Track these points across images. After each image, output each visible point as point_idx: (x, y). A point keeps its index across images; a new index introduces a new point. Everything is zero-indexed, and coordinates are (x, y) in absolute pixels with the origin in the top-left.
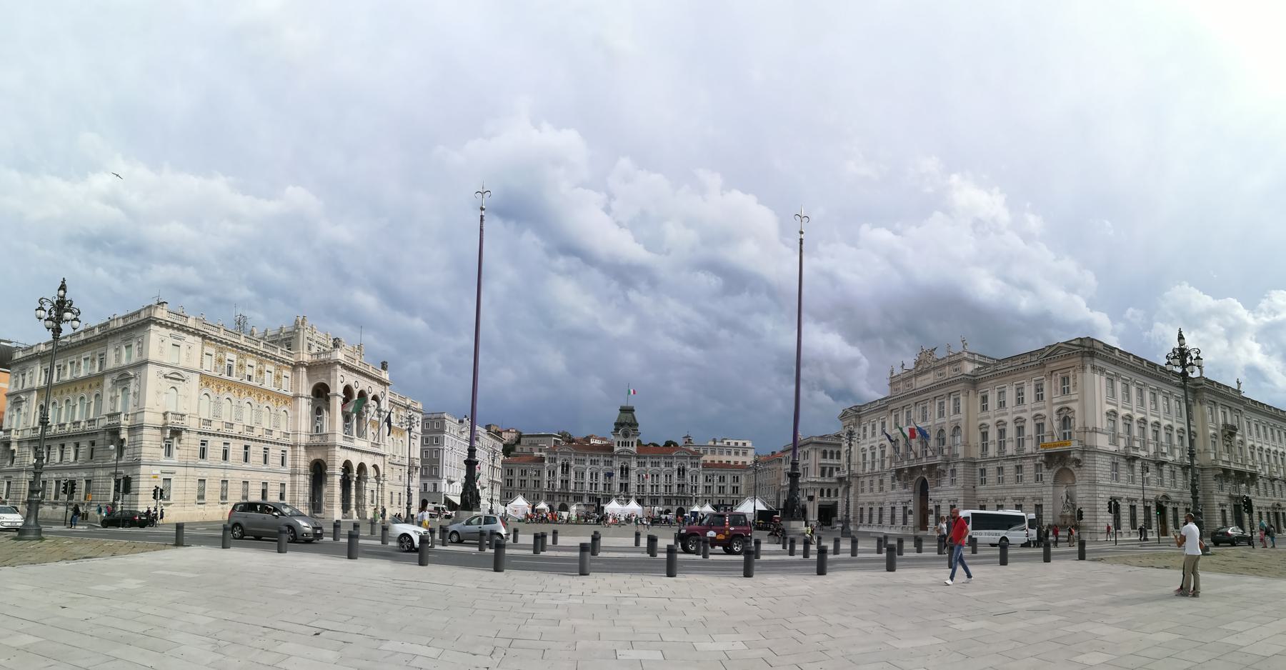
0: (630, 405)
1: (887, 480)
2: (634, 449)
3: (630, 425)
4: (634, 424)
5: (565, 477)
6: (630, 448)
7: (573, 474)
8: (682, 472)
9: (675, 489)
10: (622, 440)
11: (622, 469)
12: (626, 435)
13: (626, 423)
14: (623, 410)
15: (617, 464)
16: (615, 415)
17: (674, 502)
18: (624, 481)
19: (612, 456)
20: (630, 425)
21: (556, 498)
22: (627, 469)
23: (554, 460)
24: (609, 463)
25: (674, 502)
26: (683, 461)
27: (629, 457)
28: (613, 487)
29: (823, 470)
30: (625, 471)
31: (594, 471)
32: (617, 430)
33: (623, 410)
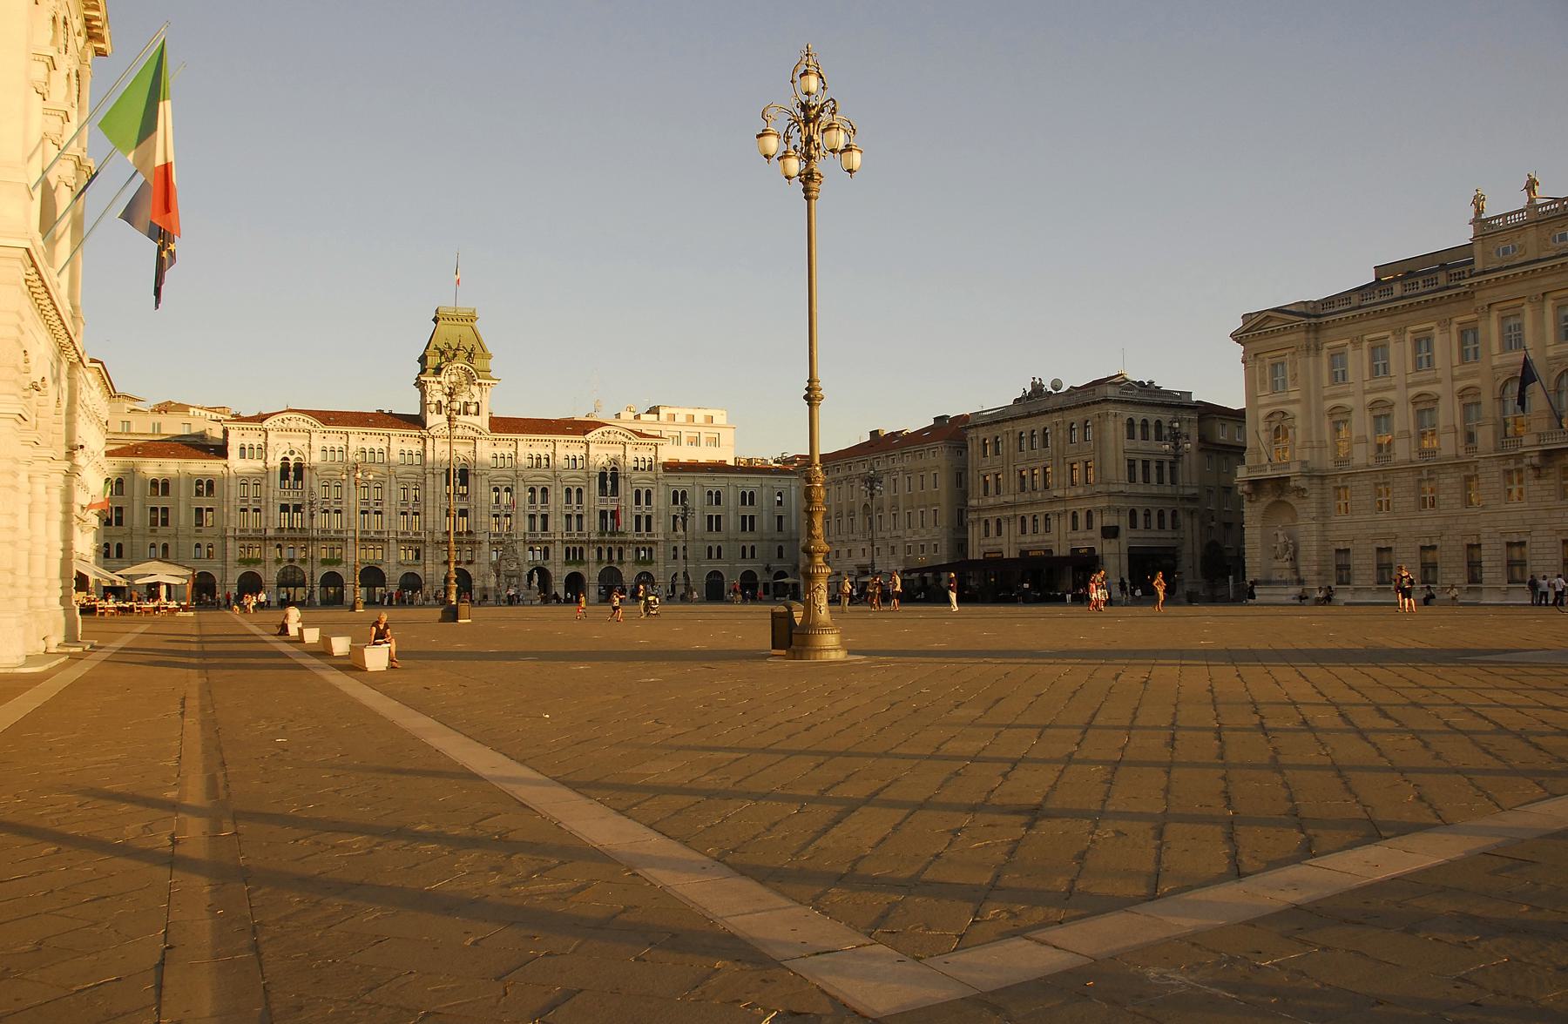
1: (1491, 476)
2: (483, 421)
9: (592, 524)
17: (591, 554)
25: (591, 554)
29: (1131, 465)
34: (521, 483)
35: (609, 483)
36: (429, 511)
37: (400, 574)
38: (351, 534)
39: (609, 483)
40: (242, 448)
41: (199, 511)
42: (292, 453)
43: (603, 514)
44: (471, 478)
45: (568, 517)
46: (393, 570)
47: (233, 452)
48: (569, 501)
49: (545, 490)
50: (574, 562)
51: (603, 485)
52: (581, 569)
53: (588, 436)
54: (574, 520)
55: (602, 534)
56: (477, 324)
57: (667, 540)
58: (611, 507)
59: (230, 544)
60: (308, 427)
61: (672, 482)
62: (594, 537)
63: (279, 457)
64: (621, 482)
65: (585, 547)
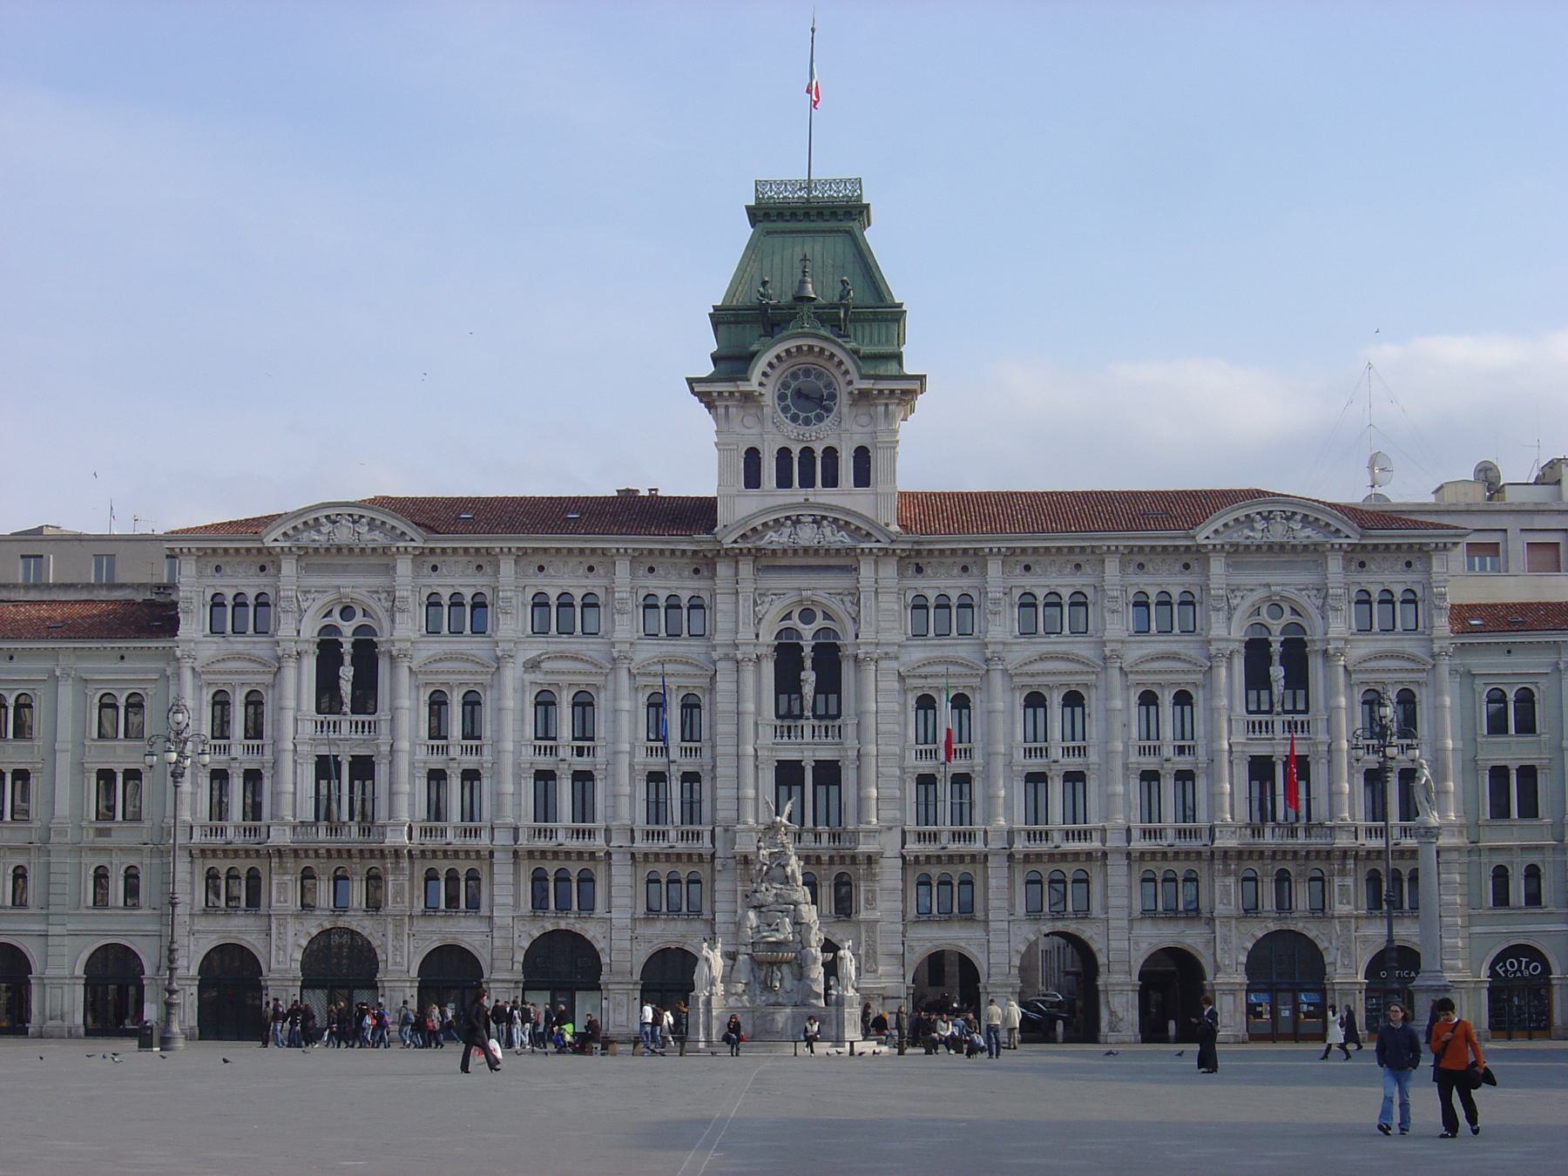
0: (831, 168)
3: (836, 319)
4: (868, 314)
5: (347, 741)
6: (845, 496)
7: (404, 703)
8: (1279, 664)
9: (1227, 801)
10: (775, 434)
11: (787, 656)
12: (809, 400)
13: (809, 311)
14: (769, 215)
15: (749, 616)
16: (715, 260)
18: (808, 750)
19: (704, 564)
20: (836, 319)
21: (282, 891)
22: (829, 658)
23: (255, 613)
24: (681, 618)
25: (1223, 894)
26: (1289, 581)
27: (843, 562)
28: (720, 797)
30: (811, 671)
31: (566, 681)
32: (731, 362)
33: (769, 215)
34: (997, 680)
35: (1277, 672)
36: (725, 769)
37: (643, 953)
38: (503, 838)
39: (1277, 672)
40: (217, 603)
41: (106, 776)
42: (347, 613)
43: (1260, 769)
44: (847, 670)
45: (1150, 777)
46: (622, 941)
47: (193, 626)
48: (1150, 731)
49: (1073, 700)
50: (1172, 914)
51: (1257, 678)
52: (1190, 937)
53: (1203, 535)
54: (1168, 786)
55: (1257, 831)
56: (875, 237)
57: (1474, 850)
58: (1277, 747)
59: (182, 868)
60: (379, 538)
61: (1482, 663)
62: (1224, 841)
63: (310, 629)
64: (1316, 666)
65: (1202, 870)
